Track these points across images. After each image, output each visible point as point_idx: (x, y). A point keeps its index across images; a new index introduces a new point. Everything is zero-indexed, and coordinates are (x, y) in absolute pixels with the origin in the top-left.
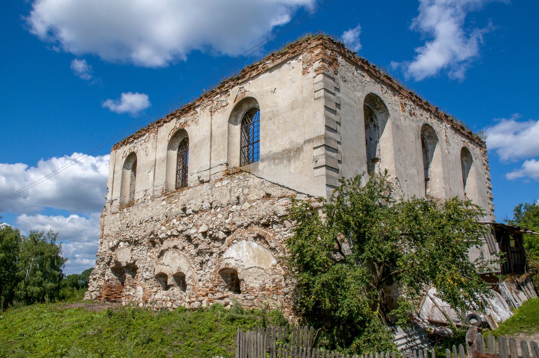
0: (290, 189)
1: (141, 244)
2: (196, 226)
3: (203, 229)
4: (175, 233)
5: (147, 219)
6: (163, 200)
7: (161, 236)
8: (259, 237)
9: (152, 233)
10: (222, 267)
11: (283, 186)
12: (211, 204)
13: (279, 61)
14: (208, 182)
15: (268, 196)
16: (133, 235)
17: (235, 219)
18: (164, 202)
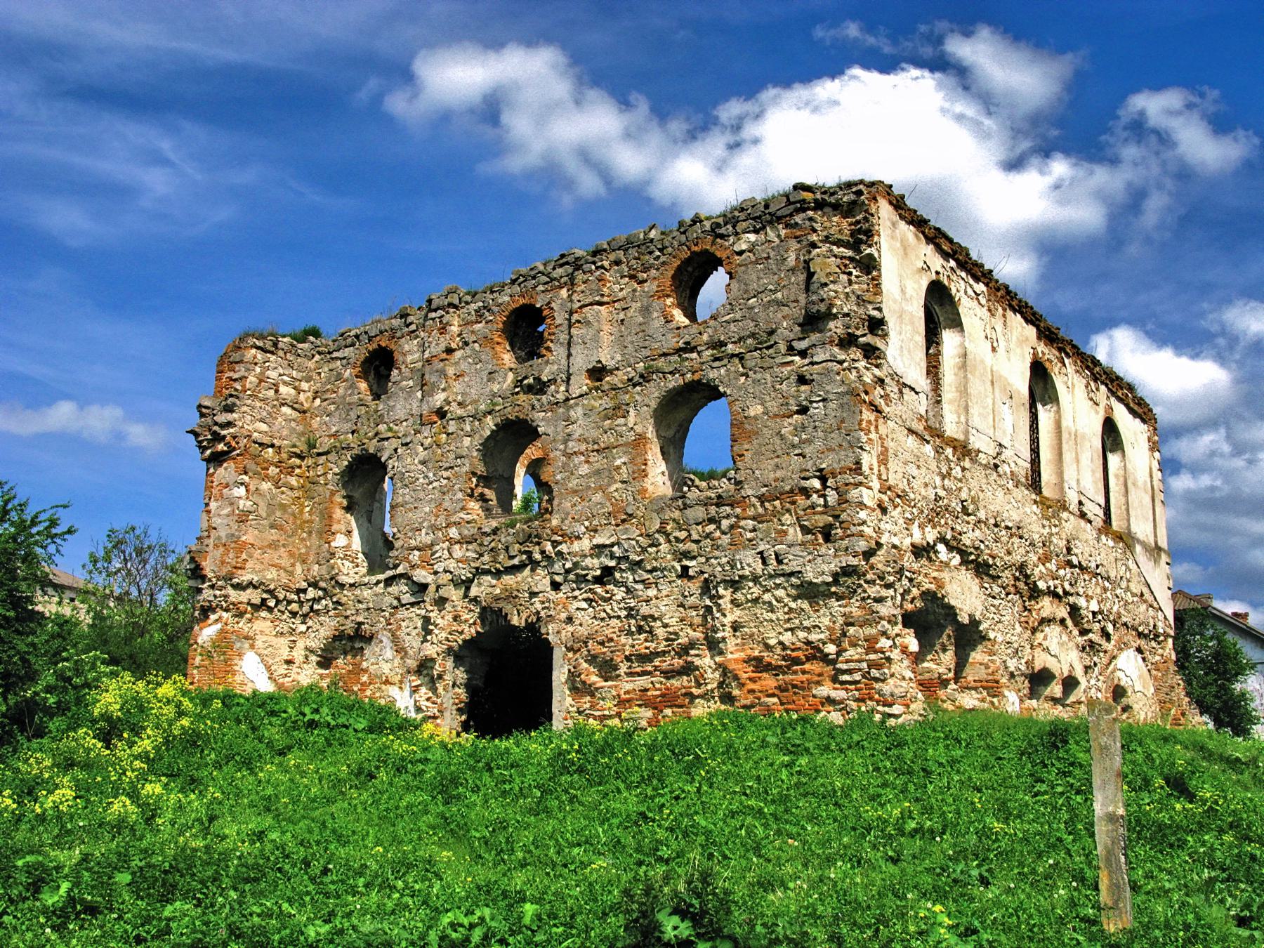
0: (1156, 600)
1: (995, 578)
2: (1088, 598)
3: (1094, 606)
4: (1061, 593)
5: (1010, 525)
6: (1035, 502)
7: (1042, 585)
8: (1139, 650)
9: (1022, 567)
10: (1116, 682)
11: (1152, 593)
12: (1098, 566)
13: (1136, 408)
14: (1090, 522)
15: (1142, 595)
16: (982, 547)
17: (1123, 612)
18: (1035, 507)
